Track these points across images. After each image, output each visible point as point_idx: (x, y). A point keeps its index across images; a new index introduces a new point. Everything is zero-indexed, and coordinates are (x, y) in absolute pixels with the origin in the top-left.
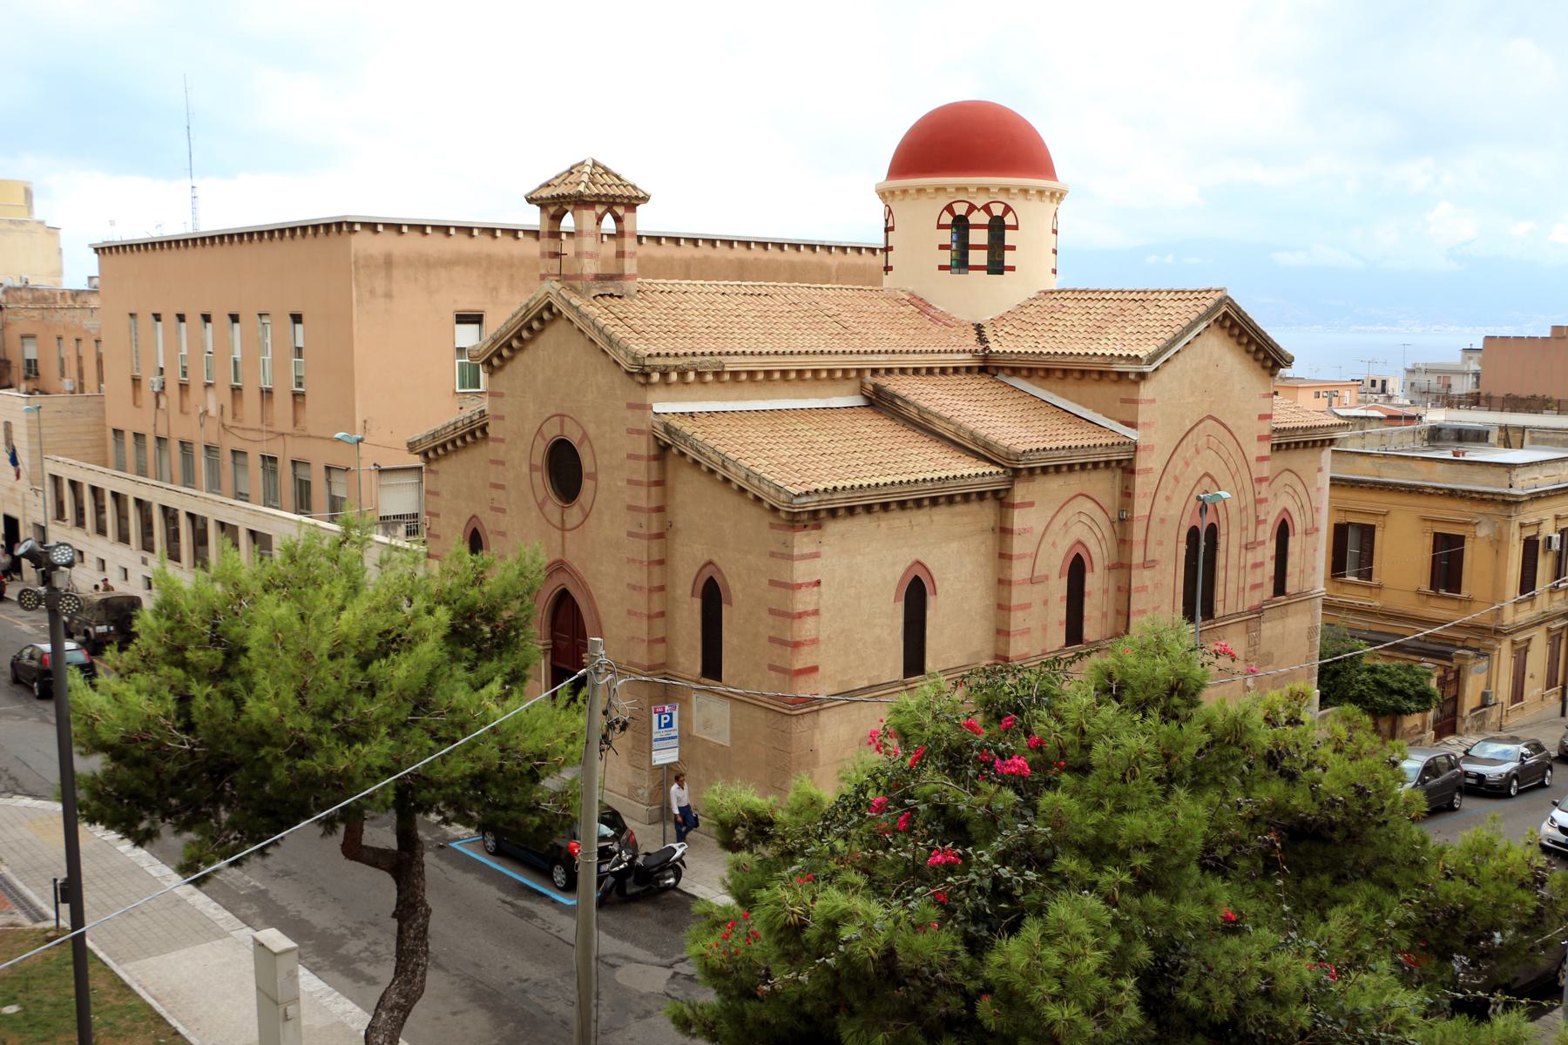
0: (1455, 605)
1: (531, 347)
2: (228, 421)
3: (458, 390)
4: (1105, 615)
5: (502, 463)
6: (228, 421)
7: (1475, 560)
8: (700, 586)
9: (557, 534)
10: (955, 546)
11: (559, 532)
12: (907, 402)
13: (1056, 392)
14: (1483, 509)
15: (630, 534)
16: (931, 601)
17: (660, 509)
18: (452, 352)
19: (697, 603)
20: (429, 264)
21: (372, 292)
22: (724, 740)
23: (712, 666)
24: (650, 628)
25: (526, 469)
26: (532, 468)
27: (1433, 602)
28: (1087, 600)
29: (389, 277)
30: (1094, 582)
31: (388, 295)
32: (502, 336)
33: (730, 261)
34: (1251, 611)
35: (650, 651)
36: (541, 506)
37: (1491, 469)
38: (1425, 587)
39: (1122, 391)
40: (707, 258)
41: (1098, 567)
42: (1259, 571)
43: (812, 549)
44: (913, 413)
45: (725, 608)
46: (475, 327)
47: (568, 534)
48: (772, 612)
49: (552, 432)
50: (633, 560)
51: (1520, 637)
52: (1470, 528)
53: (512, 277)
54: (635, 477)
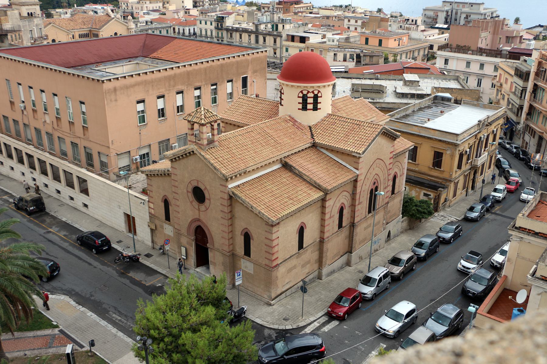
0: (439, 172)
2: (56, 127)
3: (139, 125)
4: (348, 219)
6: (56, 127)
7: (445, 159)
8: (243, 233)
9: (197, 211)
10: (311, 215)
12: (295, 169)
13: (335, 155)
14: (449, 146)
15: (222, 218)
16: (305, 231)
17: (231, 212)
18: (136, 113)
19: (243, 237)
20: (127, 87)
21: (111, 100)
23: (247, 252)
24: (229, 242)
26: (188, 192)
27: (433, 170)
28: (344, 217)
29: (116, 94)
30: (345, 212)
31: (116, 100)
33: (219, 65)
34: (385, 204)
35: (229, 248)
36: (191, 202)
37: (452, 135)
38: (431, 166)
39: (355, 159)
40: (211, 66)
41: (347, 208)
42: (388, 193)
43: (277, 230)
44: (297, 172)
46: (143, 104)
48: (266, 245)
51: (456, 181)
52: (445, 151)
53: (153, 86)
54: (223, 204)
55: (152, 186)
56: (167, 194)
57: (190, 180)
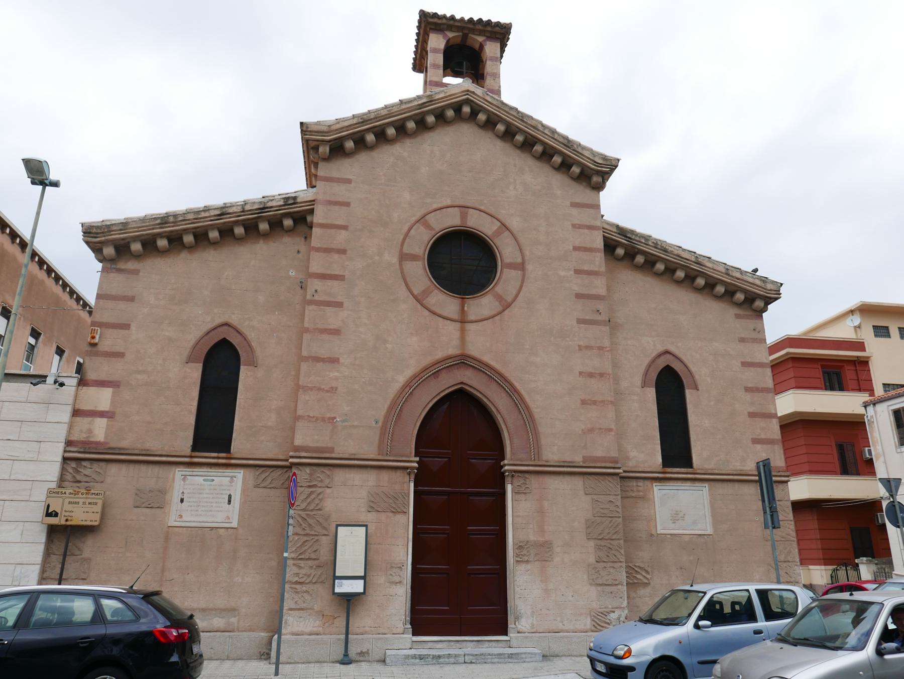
1: (408, 143)
5: (343, 252)
8: (654, 376)
9: (451, 330)
11: (458, 325)
15: (580, 321)
19: (651, 394)
22: (706, 527)
26: (404, 257)
32: (378, 118)
45: (689, 395)
47: (471, 327)
48: (748, 390)
49: (451, 221)
50: (588, 347)
55: (131, 299)
56: (234, 320)
57: (419, 214)
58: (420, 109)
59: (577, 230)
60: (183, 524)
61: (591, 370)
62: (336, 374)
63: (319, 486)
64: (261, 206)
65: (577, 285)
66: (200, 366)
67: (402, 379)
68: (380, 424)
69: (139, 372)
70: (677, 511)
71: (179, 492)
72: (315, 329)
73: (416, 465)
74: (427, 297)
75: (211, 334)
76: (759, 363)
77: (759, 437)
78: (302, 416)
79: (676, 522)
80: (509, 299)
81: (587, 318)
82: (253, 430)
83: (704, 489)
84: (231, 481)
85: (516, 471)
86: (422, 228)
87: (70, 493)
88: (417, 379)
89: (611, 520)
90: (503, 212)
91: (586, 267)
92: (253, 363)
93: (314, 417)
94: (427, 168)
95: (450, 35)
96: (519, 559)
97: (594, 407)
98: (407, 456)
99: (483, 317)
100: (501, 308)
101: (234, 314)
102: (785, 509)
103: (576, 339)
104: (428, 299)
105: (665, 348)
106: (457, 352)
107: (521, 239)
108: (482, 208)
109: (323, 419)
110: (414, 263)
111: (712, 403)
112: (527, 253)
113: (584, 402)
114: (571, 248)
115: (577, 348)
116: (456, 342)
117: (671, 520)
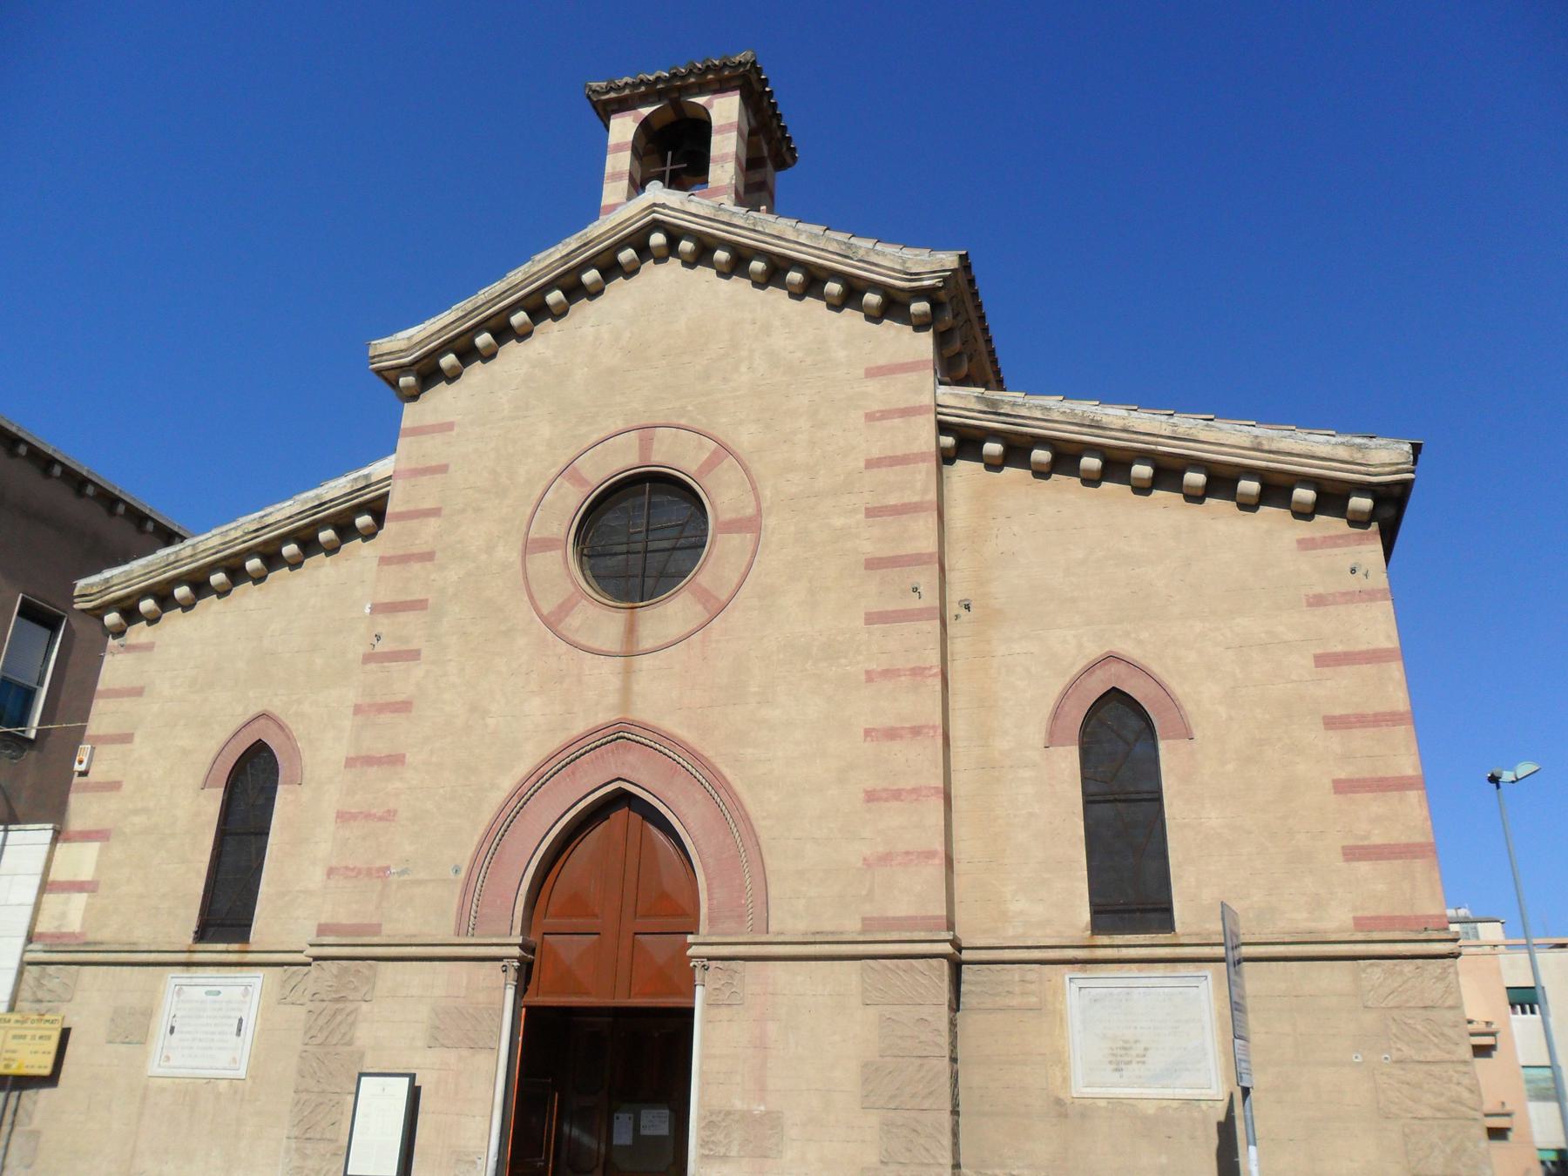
5: (428, 556)
9: (606, 672)
19: (1069, 759)
25: (509, 553)
47: (644, 662)
48: (1332, 723)
50: (888, 673)
56: (276, 706)
58: (566, 264)
59: (877, 423)
60: (169, 1072)
61: (889, 721)
62: (398, 784)
63: (351, 998)
64: (317, 503)
65: (870, 542)
66: (218, 794)
67: (508, 783)
68: (463, 874)
69: (136, 812)
70: (1126, 1042)
71: (169, 1015)
72: (370, 706)
73: (516, 951)
74: (566, 616)
75: (241, 734)
76: (1367, 652)
77: (1366, 843)
78: (337, 868)
79: (1123, 1066)
80: (724, 597)
81: (890, 607)
82: (287, 898)
83: (1203, 985)
84: (246, 993)
85: (710, 959)
86: (567, 484)
87: (17, 1021)
88: (534, 779)
89: (921, 1065)
90: (723, 420)
91: (892, 500)
92: (297, 780)
93: (353, 869)
94: (586, 369)
95: (646, 111)
96: (707, 1152)
97: (895, 804)
98: (504, 936)
99: (668, 640)
100: (707, 616)
101: (276, 695)
102: (1446, 1030)
103: (861, 658)
104: (567, 620)
105: (1107, 649)
106: (613, 717)
107: (757, 468)
108: (683, 422)
109: (369, 872)
110: (548, 554)
111: (1230, 767)
112: (767, 493)
113: (871, 797)
114: (862, 464)
115: (863, 677)
116: (613, 699)
117: (1110, 1062)
